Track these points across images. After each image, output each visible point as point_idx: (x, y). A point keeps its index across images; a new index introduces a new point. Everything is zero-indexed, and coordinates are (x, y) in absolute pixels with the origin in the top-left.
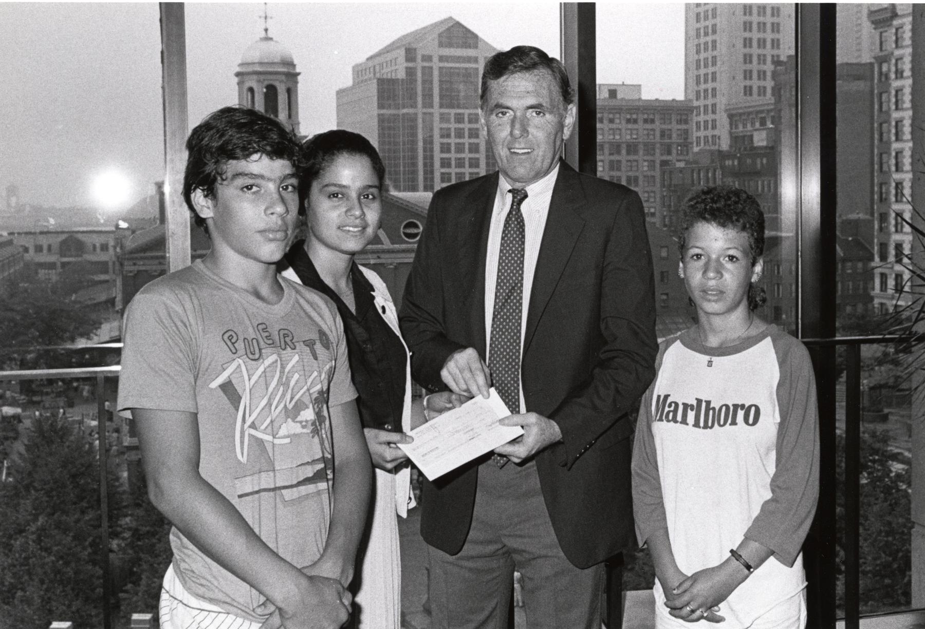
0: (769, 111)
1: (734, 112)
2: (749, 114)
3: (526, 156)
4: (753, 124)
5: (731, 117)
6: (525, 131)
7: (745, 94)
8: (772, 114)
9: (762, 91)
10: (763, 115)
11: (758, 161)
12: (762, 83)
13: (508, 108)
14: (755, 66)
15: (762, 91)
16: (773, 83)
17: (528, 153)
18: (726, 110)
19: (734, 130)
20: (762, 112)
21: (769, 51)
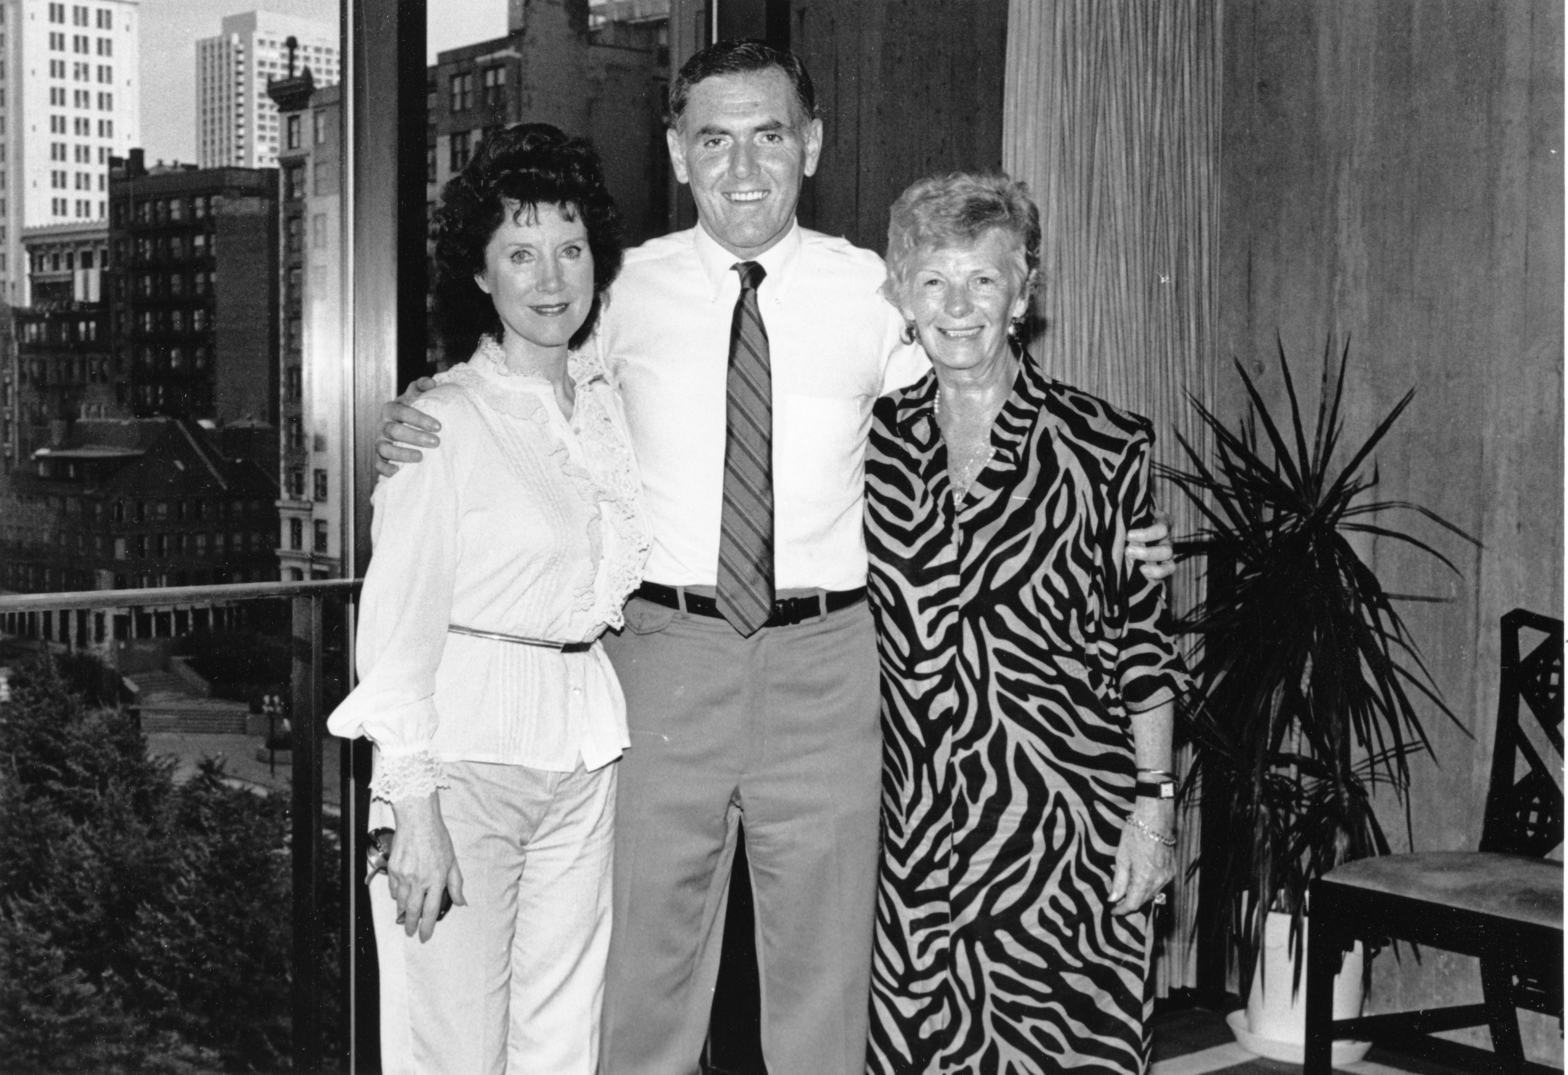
0: (98, 242)
1: (37, 241)
2: (64, 245)
3: (752, 207)
4: (70, 266)
5: (32, 249)
6: (752, 164)
7: (55, 211)
8: (104, 247)
9: (84, 207)
10: (88, 249)
11: (82, 326)
12: (83, 195)
13: (724, 132)
14: (71, 166)
15: (84, 207)
16: (105, 196)
17: (758, 200)
18: (23, 239)
19: (37, 273)
20: (85, 243)
21: (94, 141)
